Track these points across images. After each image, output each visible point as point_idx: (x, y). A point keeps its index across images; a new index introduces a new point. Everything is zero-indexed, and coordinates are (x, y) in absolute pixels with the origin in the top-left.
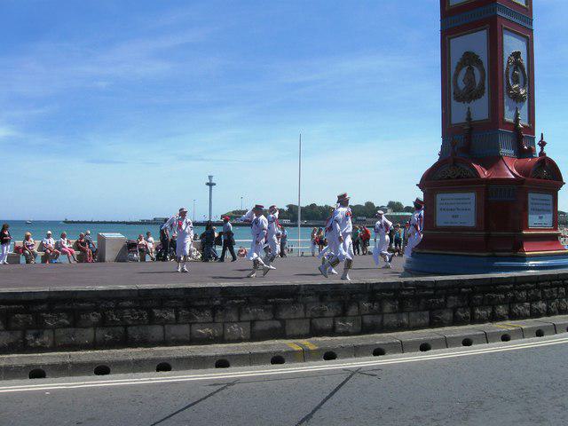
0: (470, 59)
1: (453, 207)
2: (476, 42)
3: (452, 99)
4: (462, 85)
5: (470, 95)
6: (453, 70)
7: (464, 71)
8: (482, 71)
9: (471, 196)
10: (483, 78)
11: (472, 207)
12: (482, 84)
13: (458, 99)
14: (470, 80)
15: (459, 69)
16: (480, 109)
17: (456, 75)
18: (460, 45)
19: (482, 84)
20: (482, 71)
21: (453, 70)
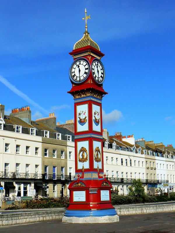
0: (83, 150)
1: (79, 195)
2: (85, 144)
3: (78, 161)
4: (81, 157)
5: (83, 160)
7: (82, 153)
12: (86, 159)
13: (80, 161)
14: (83, 155)
15: (81, 151)
17: (79, 153)
18: (80, 145)
19: (86, 159)
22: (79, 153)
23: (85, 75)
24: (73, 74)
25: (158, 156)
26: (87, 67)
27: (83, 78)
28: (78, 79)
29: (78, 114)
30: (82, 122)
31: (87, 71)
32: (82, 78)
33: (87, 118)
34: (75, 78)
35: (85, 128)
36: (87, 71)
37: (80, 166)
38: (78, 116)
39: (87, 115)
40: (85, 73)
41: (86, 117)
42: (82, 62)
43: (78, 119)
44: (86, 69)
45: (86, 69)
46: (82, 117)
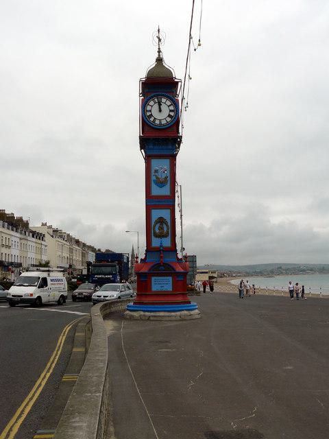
0: (161, 221)
2: (165, 214)
3: (153, 237)
4: (157, 231)
5: (161, 236)
6: (153, 224)
8: (167, 225)
9: (170, 279)
10: (168, 229)
11: (171, 282)
13: (156, 236)
15: (156, 223)
16: (166, 242)
17: (155, 226)
20: (167, 225)
21: (153, 224)
22: (155, 226)
23: (169, 119)
24: (148, 114)
25: (12, 230)
26: (172, 108)
27: (166, 122)
28: (157, 122)
29: (153, 171)
30: (161, 184)
31: (172, 114)
32: (164, 122)
33: (168, 179)
34: (152, 119)
35: (165, 191)
36: (172, 114)
37: (156, 243)
38: (153, 173)
39: (167, 173)
40: (169, 116)
41: (166, 178)
42: (164, 100)
43: (153, 178)
44: (171, 111)
45: (171, 111)
46: (162, 176)
